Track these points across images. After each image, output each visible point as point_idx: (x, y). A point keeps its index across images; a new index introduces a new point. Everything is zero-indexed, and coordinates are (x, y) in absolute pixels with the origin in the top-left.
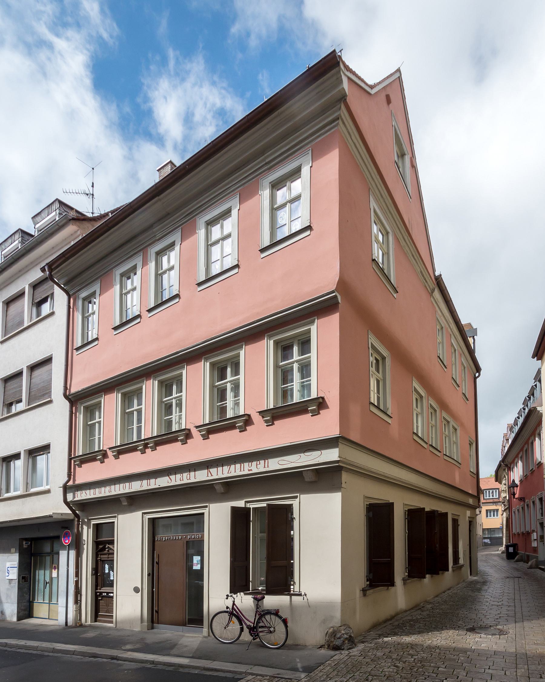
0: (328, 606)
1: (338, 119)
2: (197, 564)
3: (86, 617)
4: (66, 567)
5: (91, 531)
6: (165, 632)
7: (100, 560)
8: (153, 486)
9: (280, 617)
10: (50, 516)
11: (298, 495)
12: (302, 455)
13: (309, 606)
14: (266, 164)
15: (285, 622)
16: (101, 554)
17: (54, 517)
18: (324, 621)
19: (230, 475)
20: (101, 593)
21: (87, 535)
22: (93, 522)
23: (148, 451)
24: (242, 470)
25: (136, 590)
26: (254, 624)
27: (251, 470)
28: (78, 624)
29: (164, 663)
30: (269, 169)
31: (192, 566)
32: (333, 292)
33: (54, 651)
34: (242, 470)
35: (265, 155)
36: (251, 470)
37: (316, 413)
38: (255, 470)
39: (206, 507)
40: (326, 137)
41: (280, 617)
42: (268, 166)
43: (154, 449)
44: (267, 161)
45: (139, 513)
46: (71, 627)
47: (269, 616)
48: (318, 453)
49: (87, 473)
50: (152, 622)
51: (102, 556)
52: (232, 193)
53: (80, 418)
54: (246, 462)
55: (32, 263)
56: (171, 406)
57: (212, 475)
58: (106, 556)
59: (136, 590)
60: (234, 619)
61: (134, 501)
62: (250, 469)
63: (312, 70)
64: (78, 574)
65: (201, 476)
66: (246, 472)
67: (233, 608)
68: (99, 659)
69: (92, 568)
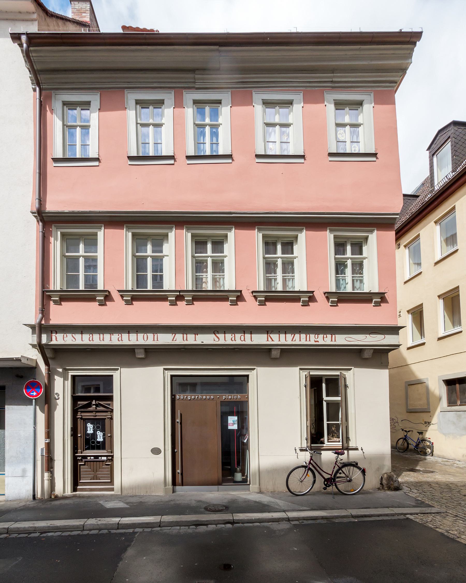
0: (380, 458)
1: (396, 83)
2: (233, 424)
3: (62, 485)
4: (32, 426)
5: (69, 383)
6: (190, 493)
7: (81, 418)
8: (248, 342)
9: (360, 469)
10: (18, 360)
11: (353, 368)
12: (368, 336)
13: (365, 458)
14: (332, 82)
15: (364, 472)
16: (82, 412)
17: (23, 361)
18: (378, 469)
19: (294, 343)
20: (85, 457)
21: (62, 388)
22: (71, 373)
23: (182, 304)
24: (308, 339)
25: (156, 451)
26: (331, 475)
27: (318, 341)
28: (52, 497)
29: (303, 517)
30: (333, 87)
31: (227, 426)
32: (397, 214)
33: (119, 526)
34: (308, 339)
35: (335, 75)
36: (318, 341)
37: (377, 304)
38: (321, 342)
39: (117, 369)
40: (386, 90)
41: (360, 469)
42: (333, 85)
43: (190, 303)
44: (334, 80)
45: (161, 368)
46: (41, 500)
47: (346, 468)
48: (383, 336)
49: (61, 314)
50: (174, 483)
51: (83, 414)
52: (293, 89)
53: (56, 245)
54: (312, 333)
55: (382, 69)
56: (276, 265)
57: (273, 341)
58: (93, 414)
59: (156, 451)
60: (310, 473)
61: (152, 355)
62: (316, 340)
63: (403, 34)
64: (49, 434)
65: (260, 339)
66: (312, 342)
67: (310, 463)
68: (246, 525)
69: (71, 428)
